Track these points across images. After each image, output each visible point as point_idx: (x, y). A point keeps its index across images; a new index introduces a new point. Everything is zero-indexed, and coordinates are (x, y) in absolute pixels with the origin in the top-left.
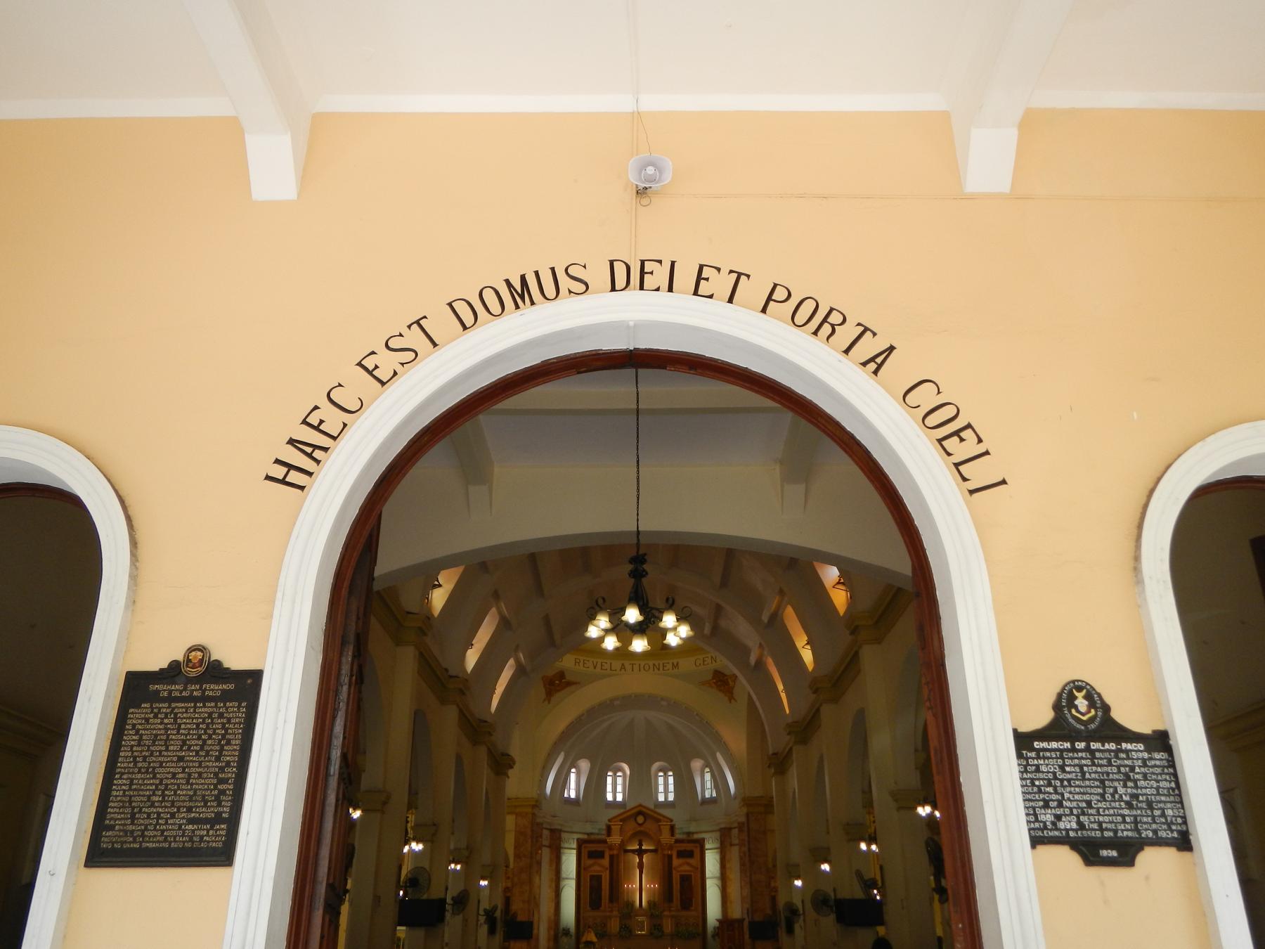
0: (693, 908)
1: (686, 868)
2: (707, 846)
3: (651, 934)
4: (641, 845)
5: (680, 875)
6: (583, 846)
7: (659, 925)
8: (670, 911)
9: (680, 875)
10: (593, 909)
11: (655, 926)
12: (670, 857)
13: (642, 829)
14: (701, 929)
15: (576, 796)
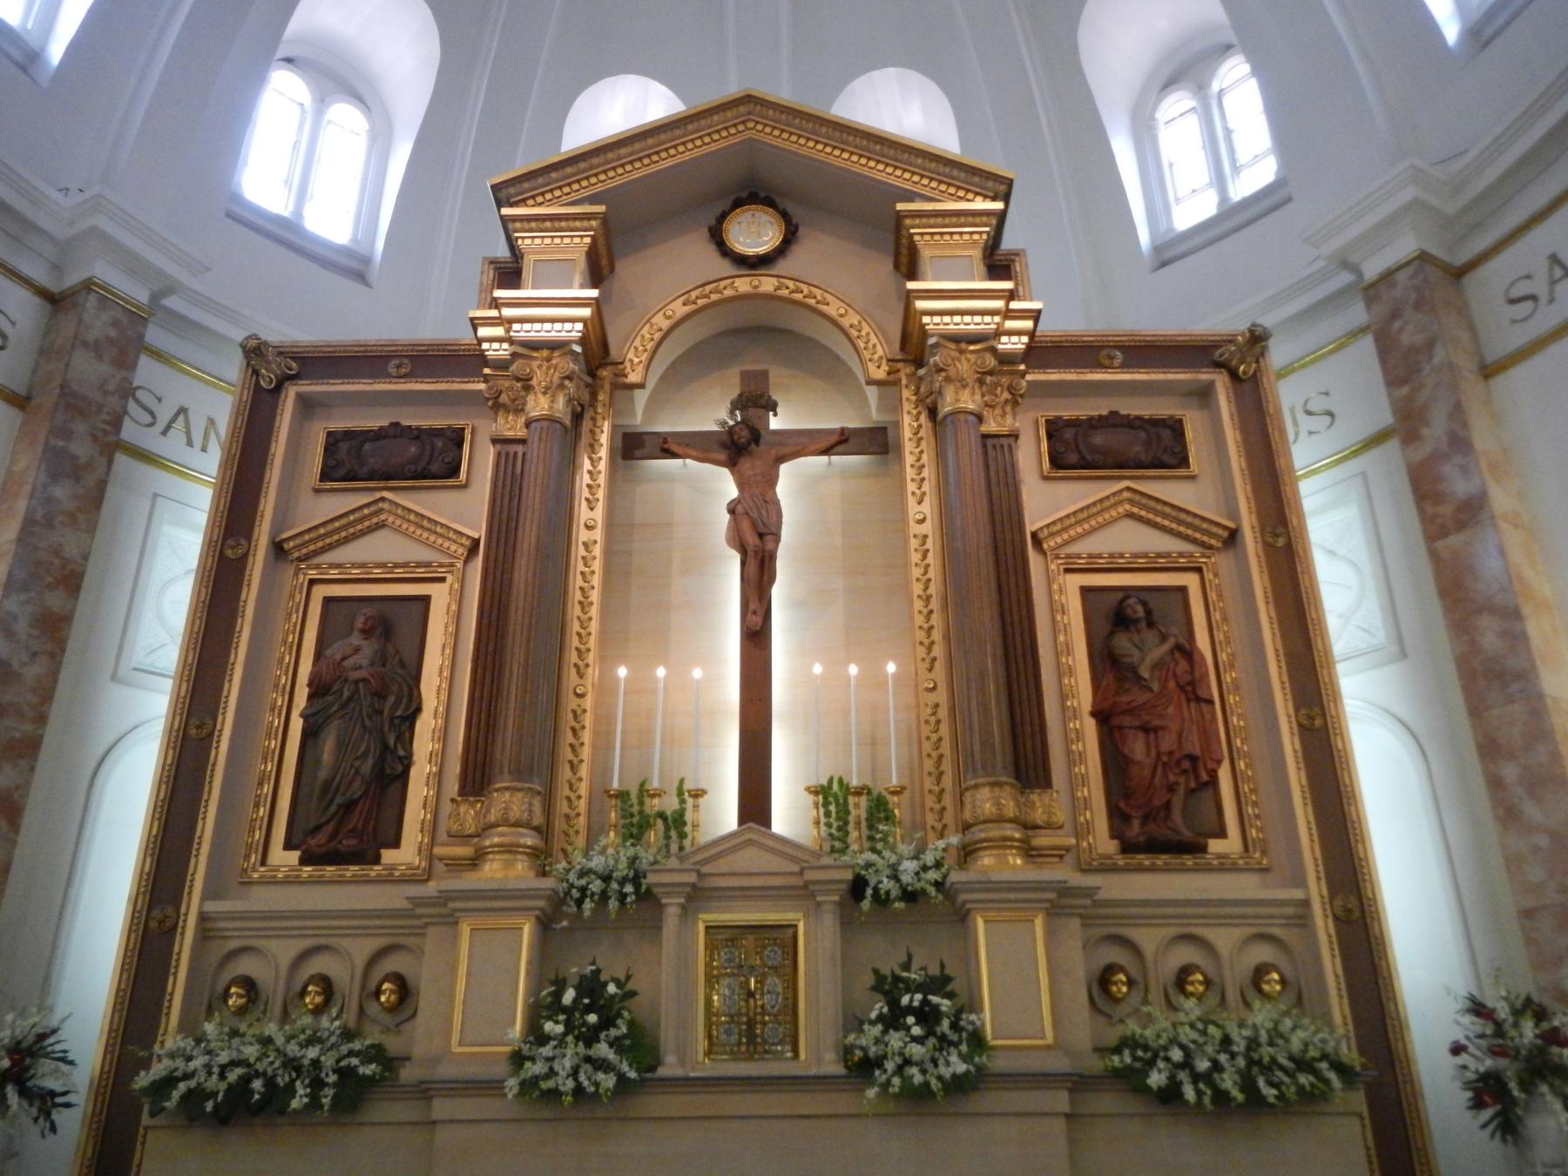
0: (1229, 845)
1: (1130, 538)
2: (1288, 395)
3: (863, 1067)
4: (755, 401)
5: (1086, 591)
6: (291, 392)
7: (940, 984)
8: (1031, 853)
9: (1086, 591)
10: (304, 861)
11: (888, 987)
12: (997, 448)
13: (768, 284)
14: (1339, 1008)
15: (354, 240)
